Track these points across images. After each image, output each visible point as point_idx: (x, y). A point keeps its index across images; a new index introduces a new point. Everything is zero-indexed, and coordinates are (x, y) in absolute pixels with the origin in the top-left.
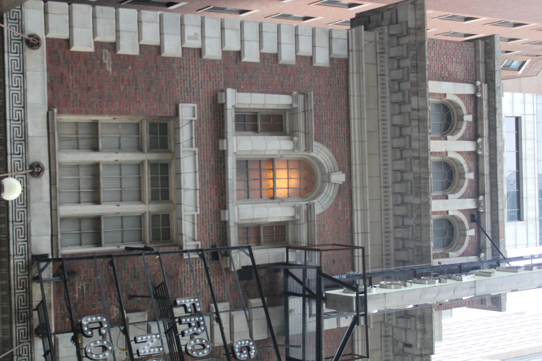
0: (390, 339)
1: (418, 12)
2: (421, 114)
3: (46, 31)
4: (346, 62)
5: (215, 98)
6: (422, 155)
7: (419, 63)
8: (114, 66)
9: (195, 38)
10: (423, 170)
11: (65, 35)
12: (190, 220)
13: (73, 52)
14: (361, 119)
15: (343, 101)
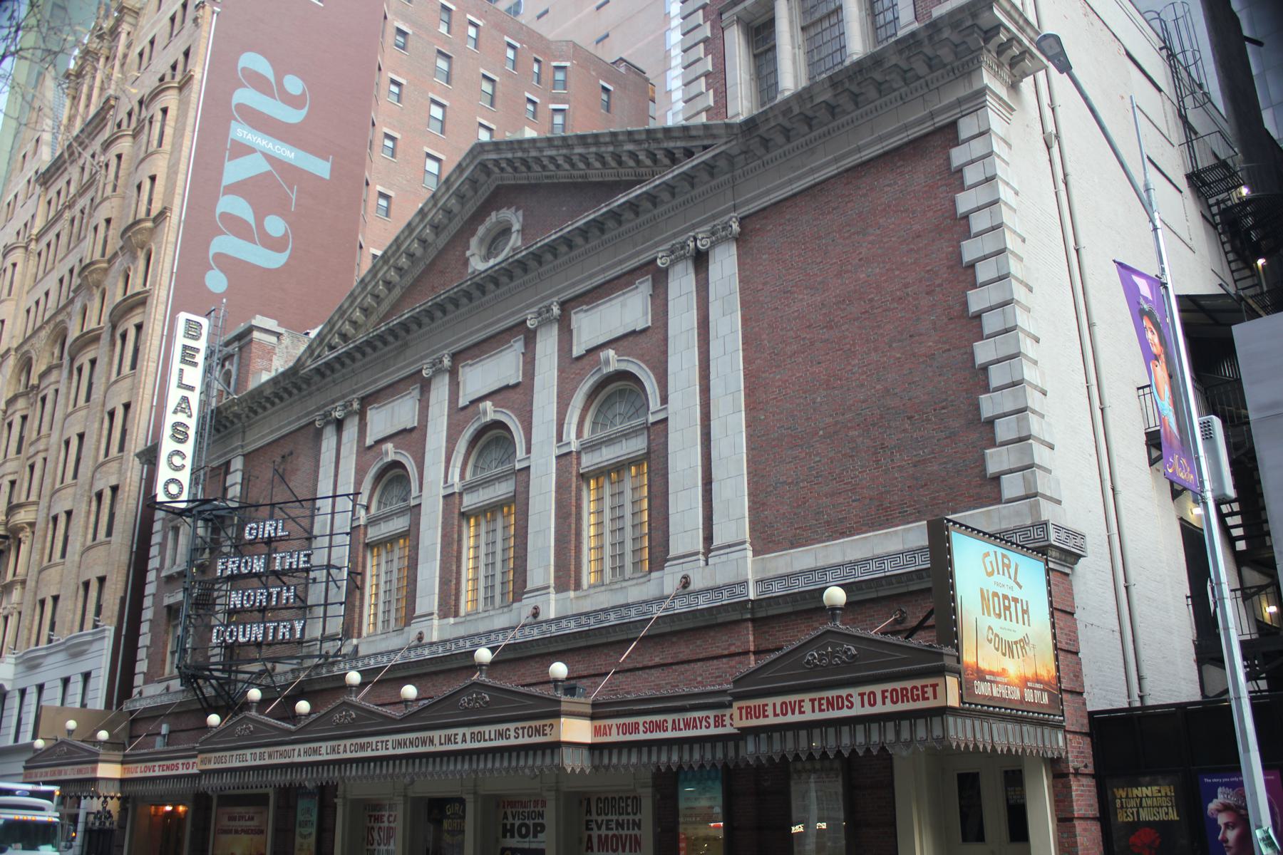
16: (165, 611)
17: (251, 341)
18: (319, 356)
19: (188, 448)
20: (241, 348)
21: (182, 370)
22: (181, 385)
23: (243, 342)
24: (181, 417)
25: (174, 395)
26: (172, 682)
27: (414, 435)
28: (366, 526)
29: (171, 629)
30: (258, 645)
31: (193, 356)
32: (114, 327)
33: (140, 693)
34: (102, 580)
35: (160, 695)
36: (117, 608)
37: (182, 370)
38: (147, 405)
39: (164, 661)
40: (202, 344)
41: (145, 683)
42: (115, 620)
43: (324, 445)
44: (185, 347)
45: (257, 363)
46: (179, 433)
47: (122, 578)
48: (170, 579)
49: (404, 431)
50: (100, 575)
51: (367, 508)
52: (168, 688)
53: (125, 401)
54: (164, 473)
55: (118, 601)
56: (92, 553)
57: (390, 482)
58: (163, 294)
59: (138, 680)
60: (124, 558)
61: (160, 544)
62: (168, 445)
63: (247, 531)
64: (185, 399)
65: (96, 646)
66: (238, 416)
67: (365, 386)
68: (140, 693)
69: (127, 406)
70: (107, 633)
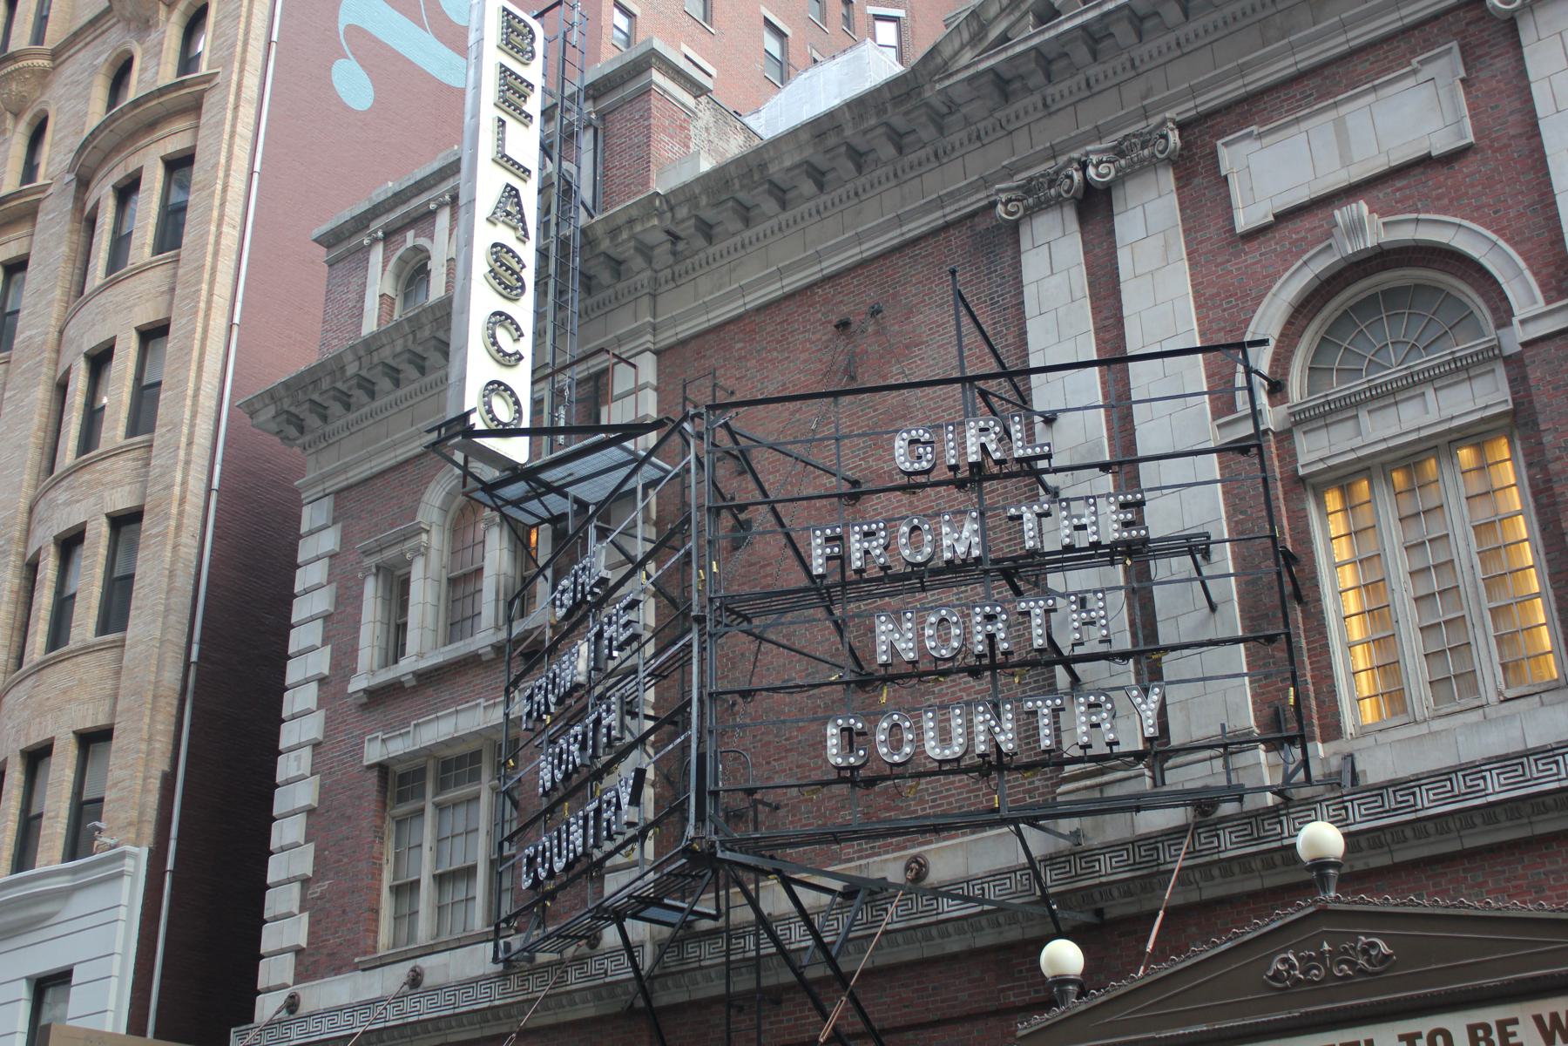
0: (677, 268)
1: (257, 406)
2: (362, 353)
3: (284, 986)
4: (338, 493)
5: (364, 707)
6: (407, 329)
7: (308, 380)
8: (324, 878)
9: (298, 759)
10: (424, 320)
11: (290, 957)
12: (490, 711)
13: (309, 944)
14: (394, 446)
15: (379, 482)
16: (373, 777)
17: (646, 91)
18: (1004, 38)
19: (523, 310)
20: (603, 116)
21: (502, 123)
22: (505, 161)
23: (605, 103)
24: (507, 236)
25: (488, 183)
26: (425, 963)
27: (1466, 168)
28: (1285, 436)
29: (390, 827)
30: (994, 764)
31: (524, 96)
32: (84, 183)
33: (292, 1005)
34: (93, 740)
35: (399, 997)
36: (153, 799)
37: (502, 123)
38: (218, 322)
39: (376, 911)
40: (533, 72)
41: (302, 976)
42: (149, 830)
43: (1033, 264)
44: (504, 70)
45: (664, 147)
46: (505, 276)
47: (164, 725)
48: (379, 697)
49: (1426, 161)
50: (88, 724)
51: (1277, 388)
52: (415, 980)
53: (147, 314)
54: (479, 368)
55: (155, 784)
56: (58, 677)
57: (1367, 306)
58: (251, 82)
59: (275, 971)
60: (171, 676)
61: (327, 618)
62: (483, 300)
63: (900, 446)
64: (512, 193)
65: (82, 903)
66: (645, 251)
67: (1193, 92)
68: (292, 1005)
69: (153, 334)
70: (129, 865)
